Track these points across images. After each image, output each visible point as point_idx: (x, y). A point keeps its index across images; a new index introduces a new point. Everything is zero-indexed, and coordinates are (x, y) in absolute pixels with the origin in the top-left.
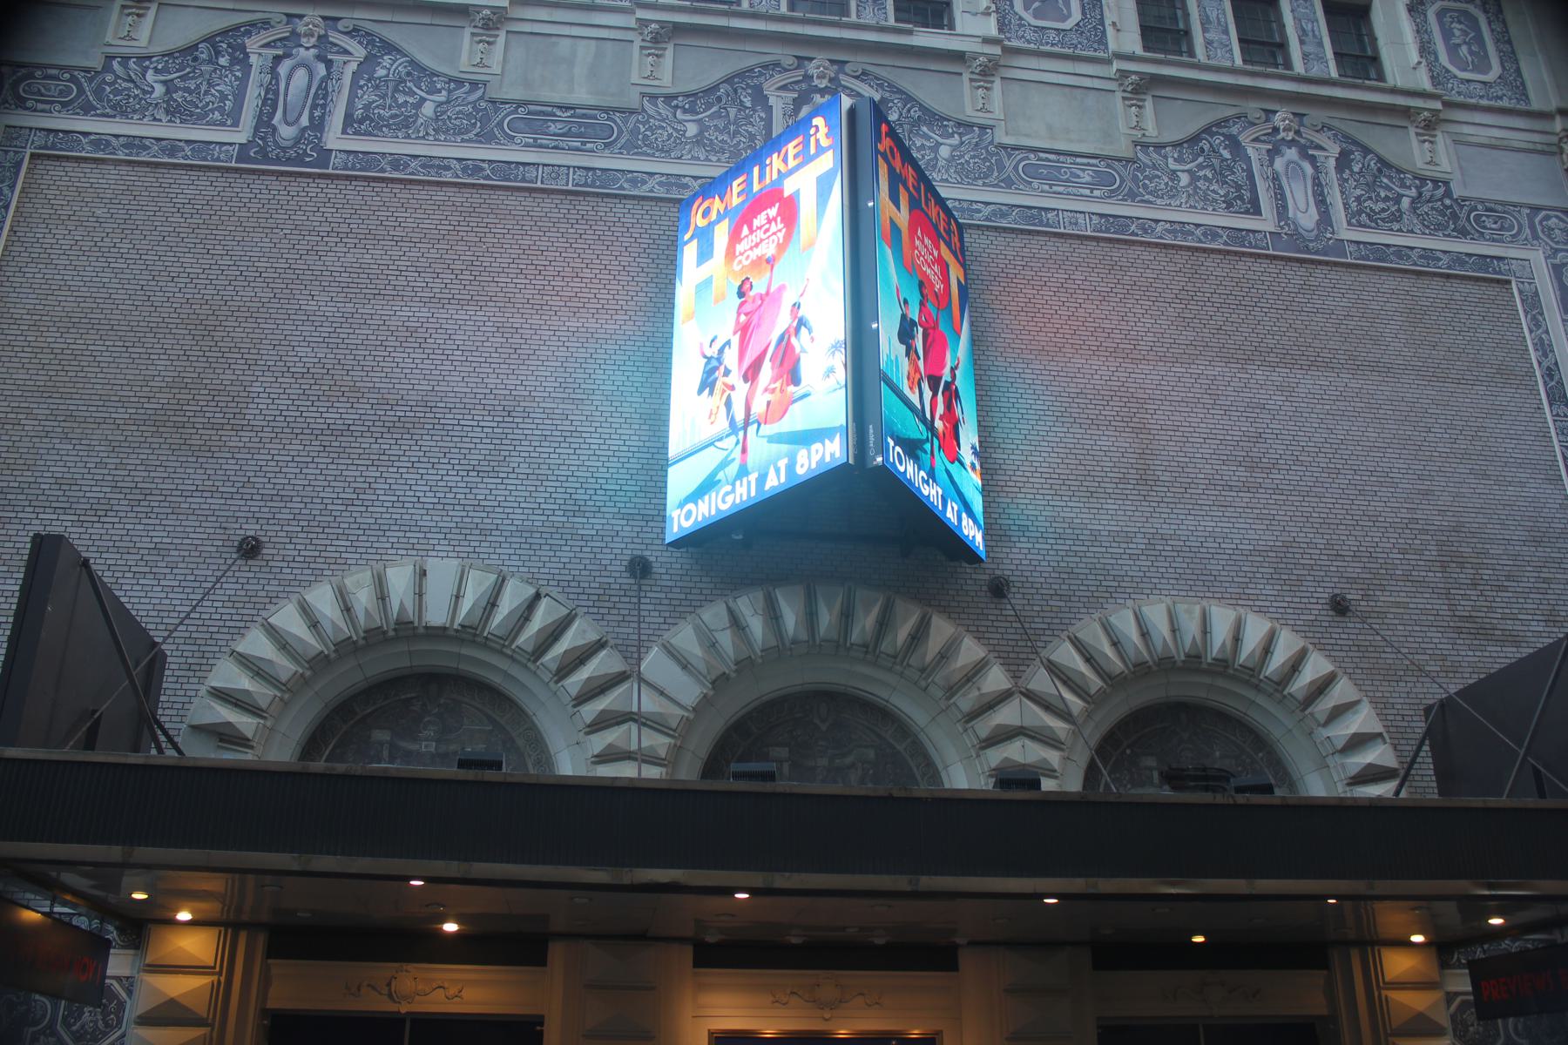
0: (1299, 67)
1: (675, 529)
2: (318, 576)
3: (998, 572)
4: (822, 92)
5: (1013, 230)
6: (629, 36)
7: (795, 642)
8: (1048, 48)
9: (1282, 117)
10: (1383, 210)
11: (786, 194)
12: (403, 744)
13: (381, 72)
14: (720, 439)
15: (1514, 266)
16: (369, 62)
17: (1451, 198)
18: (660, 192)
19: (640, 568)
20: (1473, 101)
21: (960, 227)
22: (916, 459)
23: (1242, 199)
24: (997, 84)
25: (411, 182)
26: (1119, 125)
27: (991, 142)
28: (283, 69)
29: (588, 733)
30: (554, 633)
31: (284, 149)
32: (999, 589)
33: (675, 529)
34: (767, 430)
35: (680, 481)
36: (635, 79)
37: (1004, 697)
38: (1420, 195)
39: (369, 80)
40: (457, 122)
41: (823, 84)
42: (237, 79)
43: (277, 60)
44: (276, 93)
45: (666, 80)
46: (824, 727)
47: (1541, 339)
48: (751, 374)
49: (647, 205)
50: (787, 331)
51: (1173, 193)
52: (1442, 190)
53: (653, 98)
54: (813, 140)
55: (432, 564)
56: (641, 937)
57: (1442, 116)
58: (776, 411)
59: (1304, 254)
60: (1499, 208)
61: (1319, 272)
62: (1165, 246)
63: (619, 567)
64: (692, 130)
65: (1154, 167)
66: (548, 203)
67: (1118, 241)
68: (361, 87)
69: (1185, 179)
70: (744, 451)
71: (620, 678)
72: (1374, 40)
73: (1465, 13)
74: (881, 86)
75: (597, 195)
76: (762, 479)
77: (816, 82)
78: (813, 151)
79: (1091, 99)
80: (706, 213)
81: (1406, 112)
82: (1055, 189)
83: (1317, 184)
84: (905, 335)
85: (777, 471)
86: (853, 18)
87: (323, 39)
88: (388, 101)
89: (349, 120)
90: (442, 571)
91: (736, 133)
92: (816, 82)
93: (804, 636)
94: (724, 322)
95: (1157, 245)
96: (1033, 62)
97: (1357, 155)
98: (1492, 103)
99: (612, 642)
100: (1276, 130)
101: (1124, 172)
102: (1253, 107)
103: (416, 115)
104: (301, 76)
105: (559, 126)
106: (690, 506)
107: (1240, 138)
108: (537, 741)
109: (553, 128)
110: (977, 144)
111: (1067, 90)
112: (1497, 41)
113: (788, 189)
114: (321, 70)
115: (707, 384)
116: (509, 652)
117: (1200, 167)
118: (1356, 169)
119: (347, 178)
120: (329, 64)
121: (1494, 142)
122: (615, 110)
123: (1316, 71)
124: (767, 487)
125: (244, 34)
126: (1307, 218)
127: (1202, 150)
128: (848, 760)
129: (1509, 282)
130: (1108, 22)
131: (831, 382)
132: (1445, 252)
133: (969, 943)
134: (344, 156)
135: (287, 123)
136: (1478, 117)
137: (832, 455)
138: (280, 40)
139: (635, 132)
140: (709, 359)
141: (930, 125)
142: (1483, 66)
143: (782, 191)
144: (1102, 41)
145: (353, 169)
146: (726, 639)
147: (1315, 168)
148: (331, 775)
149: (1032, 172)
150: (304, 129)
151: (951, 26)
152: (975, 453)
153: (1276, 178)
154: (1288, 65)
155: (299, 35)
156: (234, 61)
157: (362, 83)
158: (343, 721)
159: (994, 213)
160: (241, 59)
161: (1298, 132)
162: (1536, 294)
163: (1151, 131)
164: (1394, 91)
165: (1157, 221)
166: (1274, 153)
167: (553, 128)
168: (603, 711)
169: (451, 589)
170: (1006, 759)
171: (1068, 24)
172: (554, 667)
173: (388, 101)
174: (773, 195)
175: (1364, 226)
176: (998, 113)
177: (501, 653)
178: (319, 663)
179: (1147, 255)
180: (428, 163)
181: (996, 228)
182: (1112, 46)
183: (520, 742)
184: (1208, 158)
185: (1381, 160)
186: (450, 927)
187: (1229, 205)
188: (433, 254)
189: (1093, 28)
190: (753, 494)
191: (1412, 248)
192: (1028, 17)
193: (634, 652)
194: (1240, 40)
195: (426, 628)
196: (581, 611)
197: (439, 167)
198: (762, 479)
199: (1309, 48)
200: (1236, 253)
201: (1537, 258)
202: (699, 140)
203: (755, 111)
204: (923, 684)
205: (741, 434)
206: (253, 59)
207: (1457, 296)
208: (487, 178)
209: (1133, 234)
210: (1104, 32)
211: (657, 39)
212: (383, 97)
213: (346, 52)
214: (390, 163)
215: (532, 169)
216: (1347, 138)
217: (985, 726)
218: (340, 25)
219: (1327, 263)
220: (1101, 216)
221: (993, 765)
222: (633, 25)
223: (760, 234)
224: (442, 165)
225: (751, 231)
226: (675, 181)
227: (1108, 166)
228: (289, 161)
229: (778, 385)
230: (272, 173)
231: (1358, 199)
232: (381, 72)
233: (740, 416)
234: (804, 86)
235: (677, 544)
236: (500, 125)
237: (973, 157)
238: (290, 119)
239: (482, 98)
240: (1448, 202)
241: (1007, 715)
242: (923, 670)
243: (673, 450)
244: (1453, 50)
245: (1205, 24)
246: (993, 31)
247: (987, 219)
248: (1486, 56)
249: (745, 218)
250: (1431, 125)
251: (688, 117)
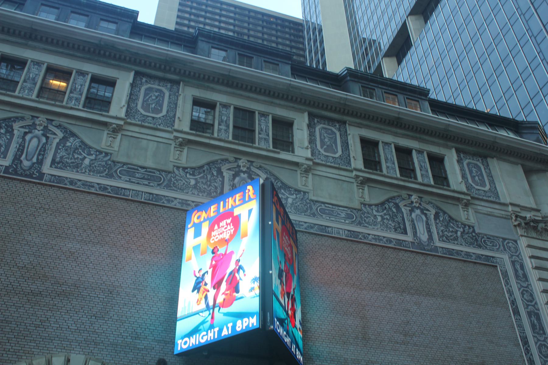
0: (420, 179)
1: (179, 349)
4: (244, 172)
5: (315, 234)
6: (170, 142)
8: (329, 164)
9: (414, 198)
10: (451, 236)
11: (235, 215)
13: (68, 144)
14: (202, 312)
15: (498, 260)
16: (64, 140)
17: (475, 233)
18: (179, 206)
20: (481, 197)
21: (296, 231)
22: (283, 326)
23: (400, 228)
24: (310, 176)
25: (77, 190)
26: (356, 196)
27: (308, 198)
28: (28, 137)
31: (24, 171)
33: (179, 349)
34: (223, 310)
35: (182, 327)
36: (171, 159)
38: (464, 231)
39: (63, 147)
40: (98, 168)
41: (244, 169)
42: (7, 139)
43: (26, 133)
44: (24, 147)
45: (183, 162)
47: (509, 289)
48: (217, 286)
49: (173, 211)
50: (233, 270)
51: (375, 223)
52: (471, 230)
53: (178, 168)
54: (247, 195)
57: (470, 202)
58: (227, 303)
59: (424, 251)
60: (492, 238)
61: (429, 258)
62: (372, 244)
64: (193, 182)
65: (368, 213)
66: (133, 206)
67: (355, 241)
68: (60, 149)
69: (379, 219)
70: (213, 318)
72: (445, 171)
73: (477, 165)
74: (267, 172)
75: (153, 204)
76: (220, 331)
77: (242, 168)
78: (247, 199)
79: (345, 185)
80: (199, 217)
81: (458, 199)
82: (331, 219)
83: (427, 224)
84: (280, 276)
85: (228, 328)
86: (257, 145)
87: (46, 128)
88: (71, 156)
89: (53, 162)
91: (210, 185)
92: (242, 168)
95: (369, 244)
96: (324, 169)
97: (441, 214)
98: (487, 198)
100: (412, 202)
101: (357, 214)
102: (404, 193)
103: (82, 164)
104: (35, 142)
105: (140, 175)
106: (186, 339)
107: (400, 204)
109: (137, 175)
110: (302, 199)
111: (336, 181)
112: (488, 176)
113: (236, 212)
114: (44, 140)
115: (197, 287)
117: (385, 214)
118: (441, 219)
119: (50, 186)
120: (47, 138)
121: (489, 213)
122: (163, 171)
123: (426, 181)
124: (223, 335)
125: (13, 121)
126: (424, 237)
127: (386, 208)
129: (497, 266)
130: (351, 156)
131: (253, 294)
132: (474, 253)
134: (50, 176)
135: (27, 160)
136: (483, 203)
137: (253, 324)
138: (28, 126)
139: (170, 180)
140: (198, 278)
141: (285, 190)
142: (485, 186)
143: (233, 213)
144: (349, 163)
145: (53, 182)
147: (427, 218)
149: (323, 211)
150: (34, 164)
151: (293, 152)
152: (300, 324)
153: (413, 221)
154: (416, 178)
155: (36, 125)
156: (7, 131)
157: (60, 147)
159: (308, 226)
160: (10, 131)
161: (420, 204)
162: (506, 271)
163: (367, 199)
164: (454, 191)
165: (369, 234)
166: (412, 211)
167: (137, 175)
171: (337, 155)
173: (71, 156)
174: (229, 214)
175: (445, 241)
176: (310, 187)
179: (365, 247)
180: (85, 184)
181: (309, 233)
182: (353, 166)
184: (388, 211)
185: (450, 217)
187: (396, 230)
188: (84, 222)
189: (346, 158)
190: (216, 337)
191: (462, 251)
192: (322, 151)
194: (399, 167)
197: (89, 186)
198: (220, 331)
199: (424, 173)
200: (398, 249)
201: (506, 257)
202: (195, 187)
203: (218, 177)
205: (211, 311)
206: (16, 132)
207: (479, 271)
208: (109, 192)
209: (360, 239)
210: (350, 160)
211: (181, 145)
212: (69, 154)
213: (55, 134)
214: (69, 182)
215: (128, 191)
216: (438, 207)
218: (54, 123)
219: (431, 255)
220: (348, 231)
222: (172, 137)
223: (223, 229)
224: (91, 185)
225: (219, 227)
226: (185, 202)
227: (351, 211)
228: (26, 176)
229: (228, 292)
230: (18, 180)
231: (442, 231)
232: (68, 144)
233: (211, 303)
234: (237, 169)
236: (116, 171)
237: (300, 204)
238: (29, 158)
239: (109, 160)
240: (474, 234)
243: (179, 314)
244: (473, 178)
245: (387, 159)
246: (309, 156)
247: (306, 229)
248: (484, 181)
249: (215, 222)
250: (467, 205)
251: (191, 177)
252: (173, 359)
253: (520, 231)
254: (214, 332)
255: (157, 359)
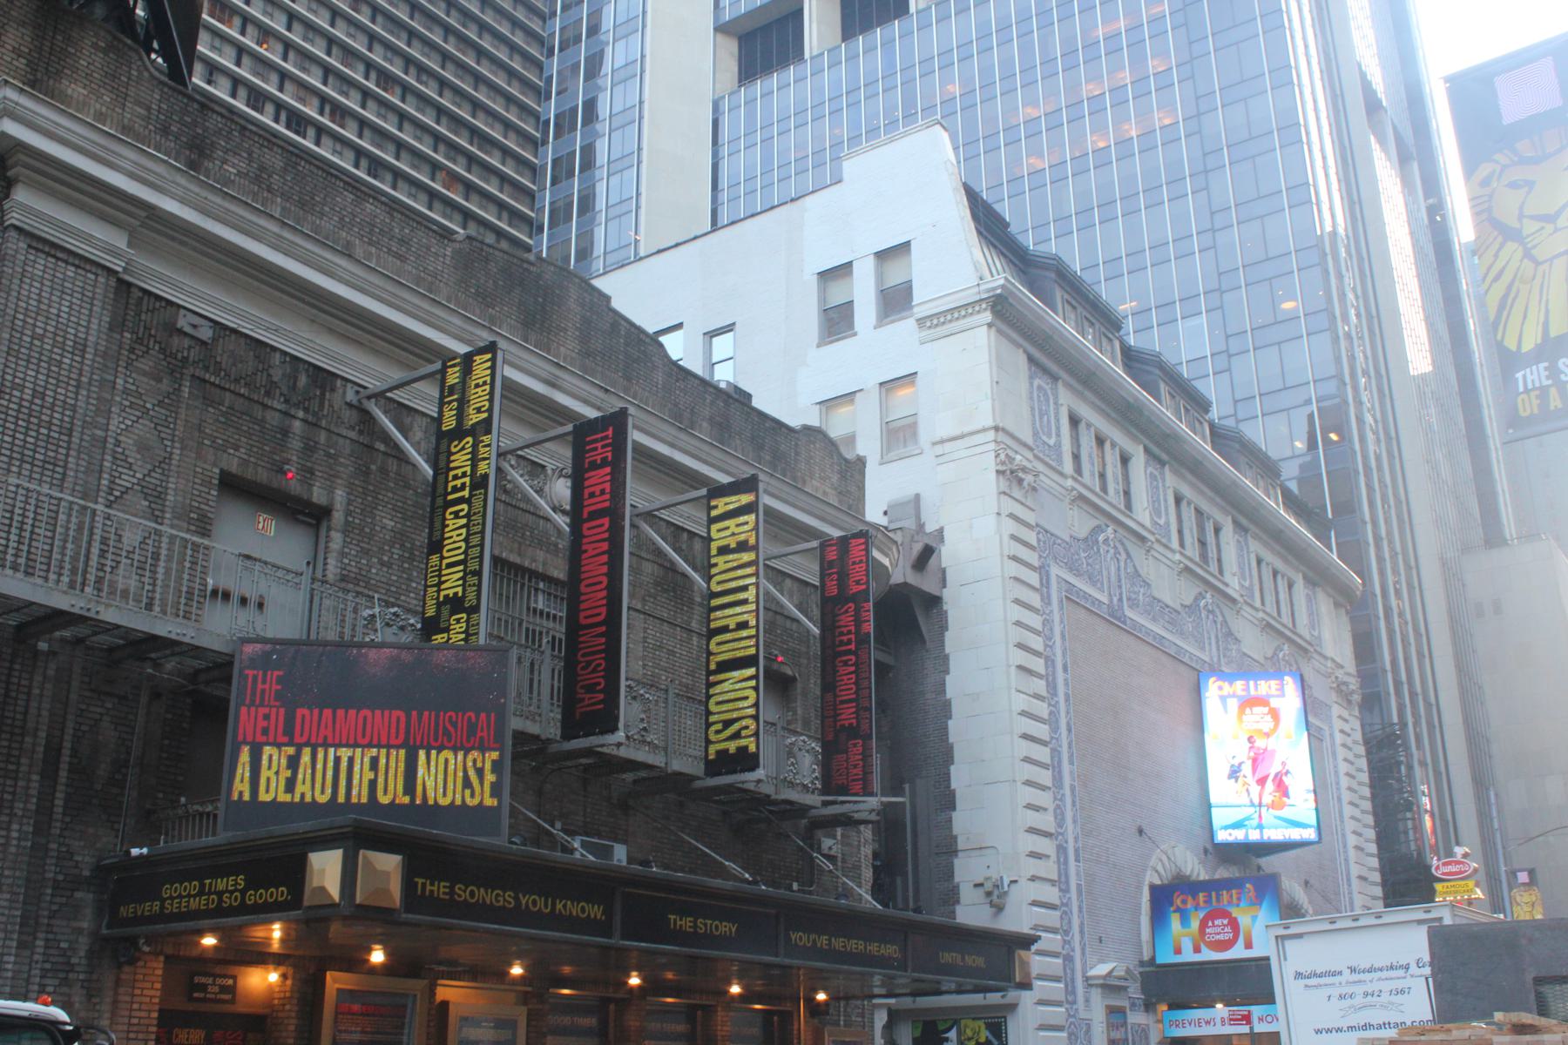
35: (1219, 817)
48: (1262, 782)
94: (1242, 754)
233: (1256, 802)
253: (1334, 696)
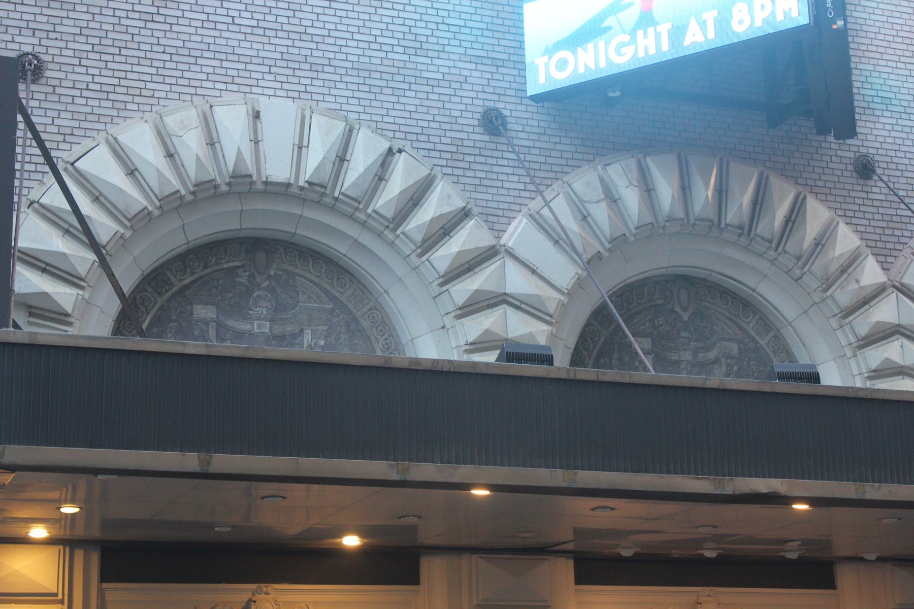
2: (121, 113)
3: (861, 149)
7: (670, 219)
12: (231, 323)
19: (493, 123)
29: (458, 317)
30: (415, 198)
32: (865, 169)
33: (542, 79)
37: (879, 292)
46: (685, 316)
55: (264, 104)
56: (543, 550)
63: (471, 120)
71: (489, 254)
76: (678, 32)
85: (702, 25)
90: (280, 115)
93: (680, 214)
99: (476, 210)
106: (565, 54)
108: (385, 325)
116: (362, 217)
124: (687, 43)
128: (711, 355)
133: (881, 560)
146: (600, 213)
148: (417, 370)
158: (154, 295)
168: (477, 292)
169: (290, 136)
170: (887, 359)
172: (419, 238)
177: (351, 217)
178: (140, 222)
183: (366, 324)
186: (351, 541)
193: (496, 221)
195: (266, 183)
196: (440, 176)
198: (678, 32)
204: (798, 273)
217: (864, 322)
221: (873, 366)
235: (538, 98)
241: (886, 311)
242: (799, 258)
252: (520, 107)
254: (658, 36)
255: (480, 110)
